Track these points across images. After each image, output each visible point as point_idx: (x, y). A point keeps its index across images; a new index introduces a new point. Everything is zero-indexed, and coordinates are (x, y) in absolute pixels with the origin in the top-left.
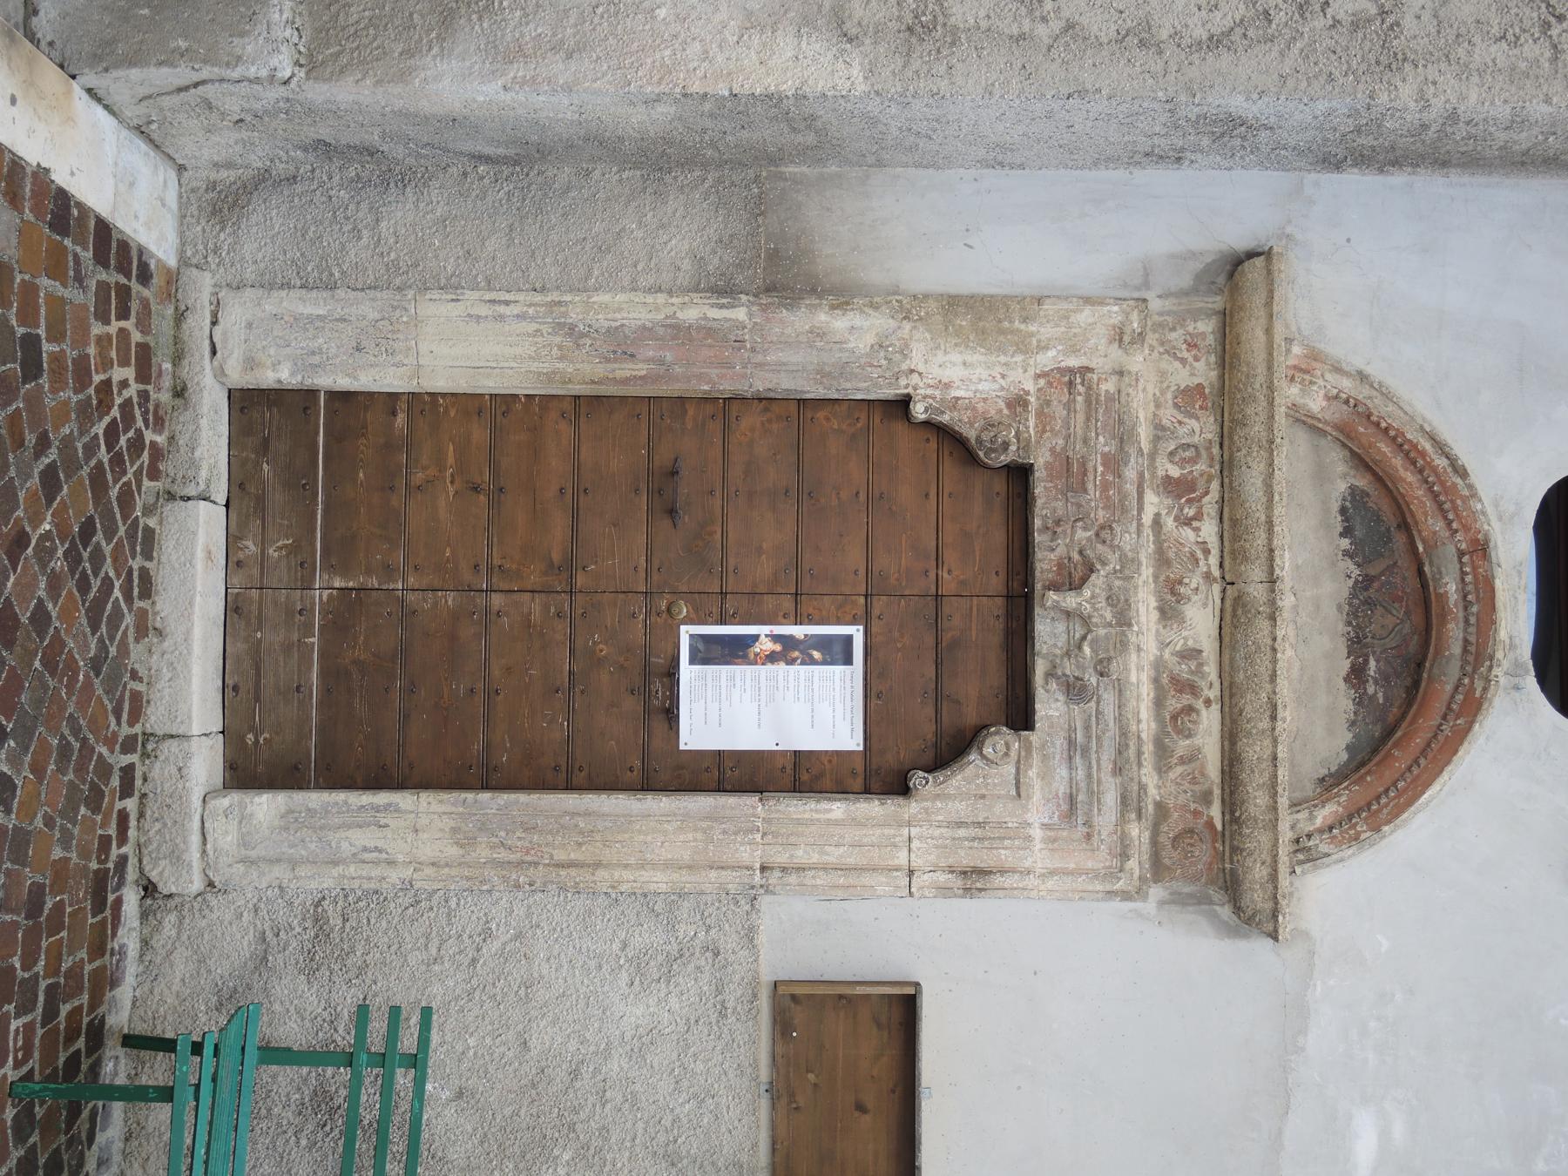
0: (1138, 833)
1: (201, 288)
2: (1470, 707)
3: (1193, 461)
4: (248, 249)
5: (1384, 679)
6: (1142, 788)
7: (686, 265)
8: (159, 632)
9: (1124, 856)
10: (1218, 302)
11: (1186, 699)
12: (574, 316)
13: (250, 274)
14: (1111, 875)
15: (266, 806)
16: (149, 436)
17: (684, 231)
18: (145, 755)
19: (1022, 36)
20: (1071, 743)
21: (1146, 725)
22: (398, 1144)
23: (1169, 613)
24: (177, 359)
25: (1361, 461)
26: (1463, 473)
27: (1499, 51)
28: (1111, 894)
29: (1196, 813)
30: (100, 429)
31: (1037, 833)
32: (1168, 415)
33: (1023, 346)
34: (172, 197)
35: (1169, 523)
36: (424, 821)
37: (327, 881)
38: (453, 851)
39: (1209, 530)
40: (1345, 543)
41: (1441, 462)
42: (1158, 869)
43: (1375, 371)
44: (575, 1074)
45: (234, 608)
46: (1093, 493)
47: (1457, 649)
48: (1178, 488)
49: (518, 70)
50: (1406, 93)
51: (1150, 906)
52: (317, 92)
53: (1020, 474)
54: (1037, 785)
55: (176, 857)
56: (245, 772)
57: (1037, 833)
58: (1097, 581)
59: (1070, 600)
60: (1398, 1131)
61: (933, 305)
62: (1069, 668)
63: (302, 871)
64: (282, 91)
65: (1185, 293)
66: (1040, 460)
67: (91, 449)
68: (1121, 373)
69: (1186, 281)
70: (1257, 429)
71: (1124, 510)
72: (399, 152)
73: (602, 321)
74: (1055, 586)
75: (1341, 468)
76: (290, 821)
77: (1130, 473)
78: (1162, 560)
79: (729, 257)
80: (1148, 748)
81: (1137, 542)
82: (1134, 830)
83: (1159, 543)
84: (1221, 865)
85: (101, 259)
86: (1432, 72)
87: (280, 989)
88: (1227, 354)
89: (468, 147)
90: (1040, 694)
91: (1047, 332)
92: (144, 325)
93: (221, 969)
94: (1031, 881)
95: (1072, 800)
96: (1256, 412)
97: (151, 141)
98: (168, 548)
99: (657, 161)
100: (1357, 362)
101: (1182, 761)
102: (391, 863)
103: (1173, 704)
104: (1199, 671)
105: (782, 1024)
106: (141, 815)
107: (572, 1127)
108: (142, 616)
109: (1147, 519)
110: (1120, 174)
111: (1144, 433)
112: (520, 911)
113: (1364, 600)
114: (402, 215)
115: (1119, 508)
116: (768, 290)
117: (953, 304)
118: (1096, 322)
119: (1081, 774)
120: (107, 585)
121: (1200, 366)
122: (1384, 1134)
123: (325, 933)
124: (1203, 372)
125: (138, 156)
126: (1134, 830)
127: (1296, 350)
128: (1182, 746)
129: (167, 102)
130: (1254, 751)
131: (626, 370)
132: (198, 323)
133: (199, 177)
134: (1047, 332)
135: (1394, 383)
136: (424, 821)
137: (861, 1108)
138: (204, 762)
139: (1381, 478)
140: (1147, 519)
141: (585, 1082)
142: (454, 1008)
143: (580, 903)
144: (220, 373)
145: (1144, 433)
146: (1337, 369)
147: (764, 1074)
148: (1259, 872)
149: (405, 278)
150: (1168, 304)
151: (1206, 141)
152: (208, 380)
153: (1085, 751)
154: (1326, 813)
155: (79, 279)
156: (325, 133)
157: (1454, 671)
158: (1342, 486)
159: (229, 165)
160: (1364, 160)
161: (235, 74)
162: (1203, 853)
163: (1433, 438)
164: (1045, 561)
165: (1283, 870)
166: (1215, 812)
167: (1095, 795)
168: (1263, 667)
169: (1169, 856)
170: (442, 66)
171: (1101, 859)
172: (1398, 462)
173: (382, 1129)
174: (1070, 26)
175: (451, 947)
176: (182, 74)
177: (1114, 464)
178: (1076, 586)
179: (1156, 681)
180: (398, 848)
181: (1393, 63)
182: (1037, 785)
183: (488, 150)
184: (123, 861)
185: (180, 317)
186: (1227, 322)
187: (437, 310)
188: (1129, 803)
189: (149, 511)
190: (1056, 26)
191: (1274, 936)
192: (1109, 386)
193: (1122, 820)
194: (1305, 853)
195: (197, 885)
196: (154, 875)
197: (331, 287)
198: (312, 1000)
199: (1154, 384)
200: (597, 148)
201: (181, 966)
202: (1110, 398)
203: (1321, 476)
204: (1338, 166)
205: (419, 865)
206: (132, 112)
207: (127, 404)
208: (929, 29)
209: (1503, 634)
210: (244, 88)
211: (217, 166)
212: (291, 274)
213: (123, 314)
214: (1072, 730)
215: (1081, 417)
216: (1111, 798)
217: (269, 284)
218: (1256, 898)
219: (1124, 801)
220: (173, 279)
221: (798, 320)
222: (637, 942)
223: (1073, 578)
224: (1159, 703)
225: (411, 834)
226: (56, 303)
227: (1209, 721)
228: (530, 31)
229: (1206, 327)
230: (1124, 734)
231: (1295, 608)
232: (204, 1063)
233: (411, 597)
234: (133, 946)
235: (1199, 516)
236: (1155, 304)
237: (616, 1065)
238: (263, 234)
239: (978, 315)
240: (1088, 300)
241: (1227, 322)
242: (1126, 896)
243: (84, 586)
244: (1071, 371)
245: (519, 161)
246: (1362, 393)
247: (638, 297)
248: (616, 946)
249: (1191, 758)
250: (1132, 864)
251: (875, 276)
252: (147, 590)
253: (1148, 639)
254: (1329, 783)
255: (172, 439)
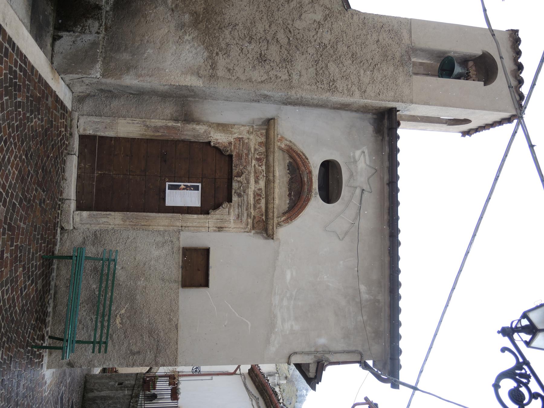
0: (250, 221)
1: (76, 115)
2: (308, 200)
3: (261, 155)
4: (85, 108)
5: (294, 196)
6: (251, 213)
7: (169, 115)
8: (66, 180)
9: (247, 225)
10: (266, 127)
11: (259, 197)
12: (148, 123)
13: (85, 113)
14: (245, 228)
15: (85, 214)
16: (66, 142)
17: (169, 109)
18: (62, 203)
19: (230, 79)
20: (239, 205)
21: (252, 201)
22: (110, 277)
23: (256, 182)
24: (71, 128)
25: (291, 157)
26: (307, 159)
27: (308, 87)
28: (245, 232)
29: (260, 218)
30: (59, 139)
31: (232, 221)
32: (257, 147)
33: (231, 133)
34: (71, 98)
35: (257, 166)
36: (116, 217)
37: (97, 228)
38: (122, 223)
39: (264, 167)
40: (288, 171)
41: (304, 157)
42: (253, 228)
43: (293, 141)
44: (145, 264)
45: (79, 177)
46: (243, 160)
47: (306, 190)
48: (258, 160)
49: (141, 79)
50: (293, 92)
51: (252, 234)
52: (104, 80)
53: (231, 156)
54: (232, 212)
55: (68, 222)
56: (79, 208)
57: (232, 221)
58: (244, 175)
59: (239, 179)
60: (294, 273)
61: (215, 125)
62: (238, 191)
63: (92, 226)
64: (97, 80)
65: (260, 125)
66: (234, 154)
67: (58, 143)
68: (249, 139)
69: (260, 123)
70: (272, 149)
71: (249, 163)
72: (116, 92)
73: (153, 125)
74: (236, 177)
75: (288, 158)
76: (90, 216)
77: (250, 157)
78: (255, 172)
79: (177, 114)
80: (252, 206)
81: (251, 169)
82: (249, 220)
83: (255, 169)
84: (264, 227)
85: (61, 108)
86: (297, 89)
87: (88, 248)
88: (267, 136)
89: (129, 91)
90: (233, 196)
91: (236, 131)
92: (66, 121)
93: (76, 244)
94: (231, 229)
95: (238, 215)
96: (272, 146)
97: (69, 88)
98: (68, 164)
99: (164, 96)
100: (290, 139)
101: (258, 208)
102: (110, 224)
103: (257, 198)
104: (261, 192)
105: (184, 255)
106: (61, 214)
107: (144, 274)
108: (63, 176)
109: (253, 165)
110: (249, 104)
111: (252, 150)
112: (135, 234)
113: (291, 182)
114: (115, 103)
115: (248, 163)
116: (185, 120)
117: (219, 125)
118: (244, 129)
119: (240, 210)
120: (59, 168)
121: (263, 138)
122: (292, 274)
123: (97, 238)
124: (263, 139)
125: (67, 90)
126: (249, 220)
127: (279, 136)
128: (258, 206)
129: (75, 80)
130: (270, 206)
131: (157, 134)
132: (75, 121)
133: (76, 95)
134: (236, 131)
135: (296, 143)
136: (116, 217)
137: (199, 270)
138: (73, 205)
139: (295, 160)
140: (253, 165)
141: (147, 266)
142: (122, 252)
143: (146, 233)
144: (79, 131)
145: (252, 150)
146: (286, 140)
147: (181, 264)
148: (271, 227)
149: (116, 115)
150: (257, 127)
151: (263, 99)
152: (76, 133)
153: (241, 206)
154: (283, 219)
155: (58, 111)
156: (103, 87)
157: (306, 194)
158: (288, 161)
159: (82, 92)
160: (290, 104)
161: (89, 76)
162: (261, 225)
163: (302, 153)
164: (235, 172)
165: (275, 227)
166: (264, 217)
167: (242, 214)
168: (272, 192)
169: (256, 225)
170: (127, 77)
171: (243, 226)
172: (297, 157)
173: (107, 275)
174: (238, 78)
175: (121, 240)
176: (80, 76)
177: (247, 155)
178: (240, 176)
179: (254, 194)
180: (111, 222)
181: (291, 88)
182: (232, 212)
183: (133, 92)
184: (58, 222)
185: (71, 120)
186: (268, 131)
187: (121, 121)
188: (249, 215)
189: (65, 156)
190: (236, 77)
191: (273, 239)
192: (246, 141)
193: (247, 218)
194: (279, 225)
195: (72, 228)
196: (63, 226)
197: (101, 116)
198: (94, 250)
199: (254, 141)
200: (153, 93)
201: (68, 244)
202: (247, 143)
203: (284, 159)
204: (286, 104)
205: (115, 225)
206: (68, 82)
207: (63, 135)
208: (214, 76)
209: (314, 187)
210: (90, 79)
211: (80, 92)
212: (93, 113)
213: (64, 119)
214: (239, 202)
215: (241, 146)
216: (245, 215)
217: (89, 115)
218: (270, 232)
219: (248, 215)
220: (71, 113)
221: (190, 126)
222: (157, 240)
223: (239, 175)
224: (254, 198)
225: (114, 220)
226: (56, 115)
227: (263, 201)
228: (143, 72)
229: (264, 131)
230: (248, 203)
231: (279, 183)
232: (75, 258)
233: (114, 176)
234: (59, 239)
235: (262, 165)
236: (255, 127)
237: (153, 262)
238: (88, 106)
239: (223, 127)
240: (243, 125)
241: (268, 131)
242: (247, 232)
243: (56, 168)
244: (240, 138)
245: (140, 95)
246: (291, 144)
247: (160, 121)
248: (153, 241)
249: (260, 208)
250: (249, 226)
251: (204, 119)
252: (64, 172)
253: (252, 186)
254: (284, 214)
255: (69, 143)
